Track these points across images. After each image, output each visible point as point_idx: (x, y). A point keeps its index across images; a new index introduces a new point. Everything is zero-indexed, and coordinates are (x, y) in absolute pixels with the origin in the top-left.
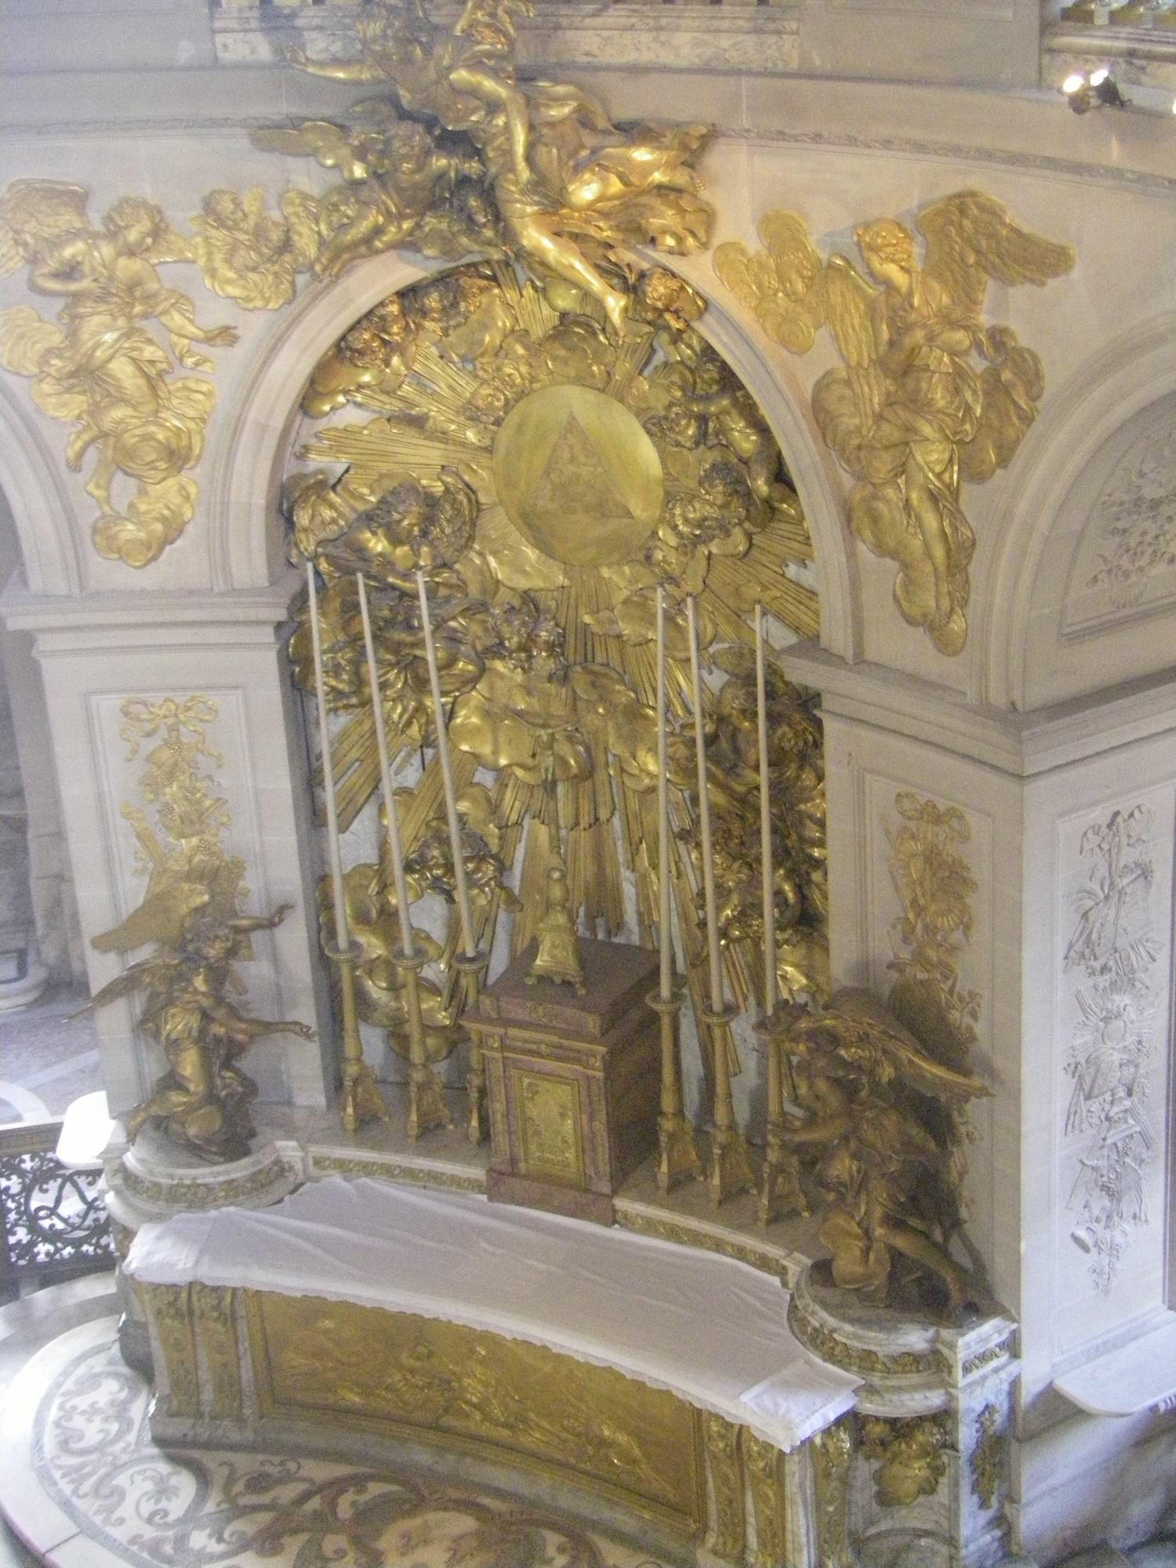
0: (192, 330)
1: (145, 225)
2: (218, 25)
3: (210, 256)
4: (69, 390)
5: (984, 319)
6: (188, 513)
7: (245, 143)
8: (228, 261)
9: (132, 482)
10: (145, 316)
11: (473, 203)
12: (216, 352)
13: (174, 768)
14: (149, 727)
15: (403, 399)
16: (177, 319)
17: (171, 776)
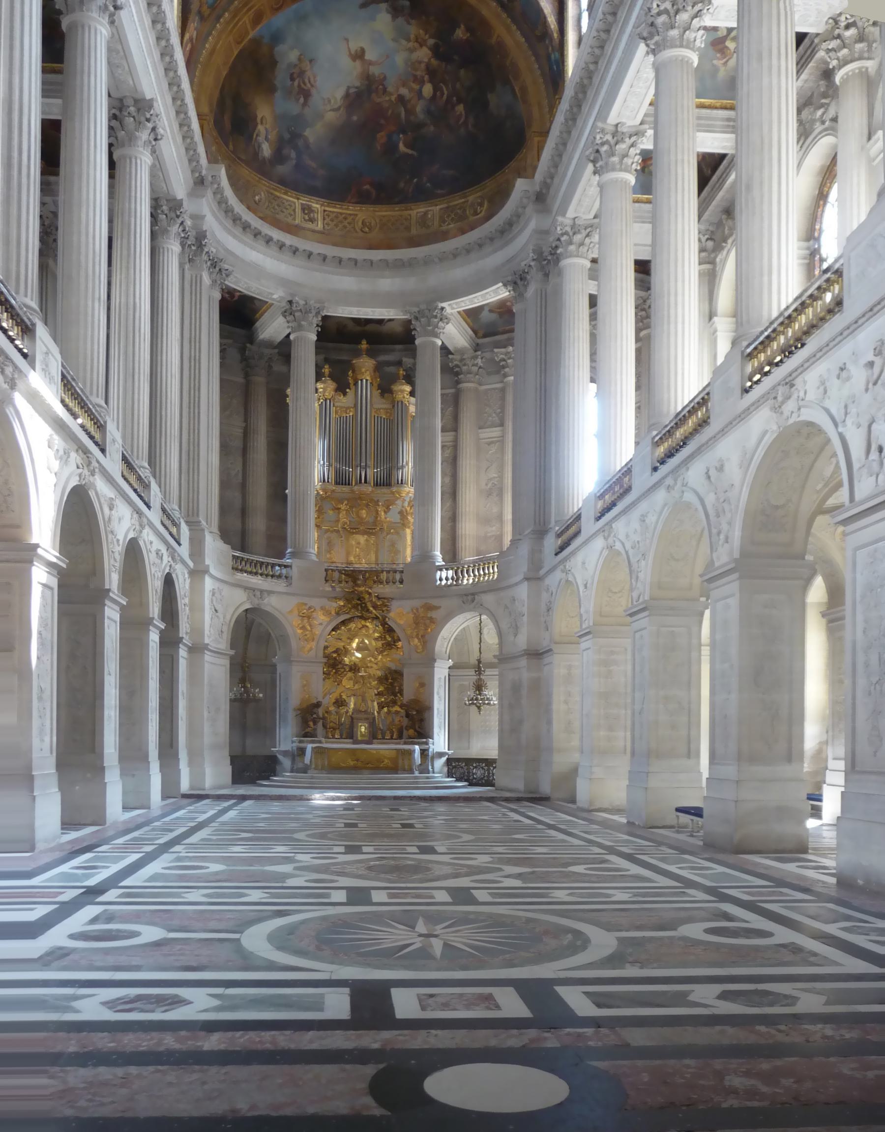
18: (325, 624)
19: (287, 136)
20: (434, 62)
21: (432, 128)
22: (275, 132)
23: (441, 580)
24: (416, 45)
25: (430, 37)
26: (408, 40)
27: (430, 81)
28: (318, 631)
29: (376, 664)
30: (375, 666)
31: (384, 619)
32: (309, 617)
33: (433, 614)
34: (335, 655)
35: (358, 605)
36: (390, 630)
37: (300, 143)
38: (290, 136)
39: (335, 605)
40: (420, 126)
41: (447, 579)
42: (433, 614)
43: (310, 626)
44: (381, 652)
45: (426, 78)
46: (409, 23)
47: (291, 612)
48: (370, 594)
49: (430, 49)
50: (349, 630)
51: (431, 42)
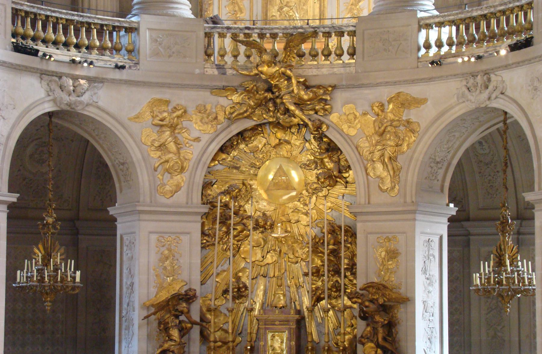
0: (189, 137)
1: (183, 110)
2: (206, 66)
3: (196, 119)
4: (157, 150)
5: (404, 118)
6: (182, 184)
7: (209, 93)
8: (201, 121)
9: (169, 175)
10: (179, 133)
11: (271, 105)
12: (195, 144)
13: (168, 258)
14: (163, 244)
15: (234, 163)
16: (186, 135)
17: (167, 258)
18: (205, 139)
23: (428, 46)
28: (192, 152)
29: (306, 214)
30: (304, 220)
31: (318, 128)
32: (173, 127)
33: (413, 115)
34: (226, 199)
36: (332, 149)
39: (223, 101)
41: (439, 45)
42: (413, 115)
43: (175, 143)
44: (316, 191)
47: (137, 117)
48: (289, 79)
50: (255, 151)
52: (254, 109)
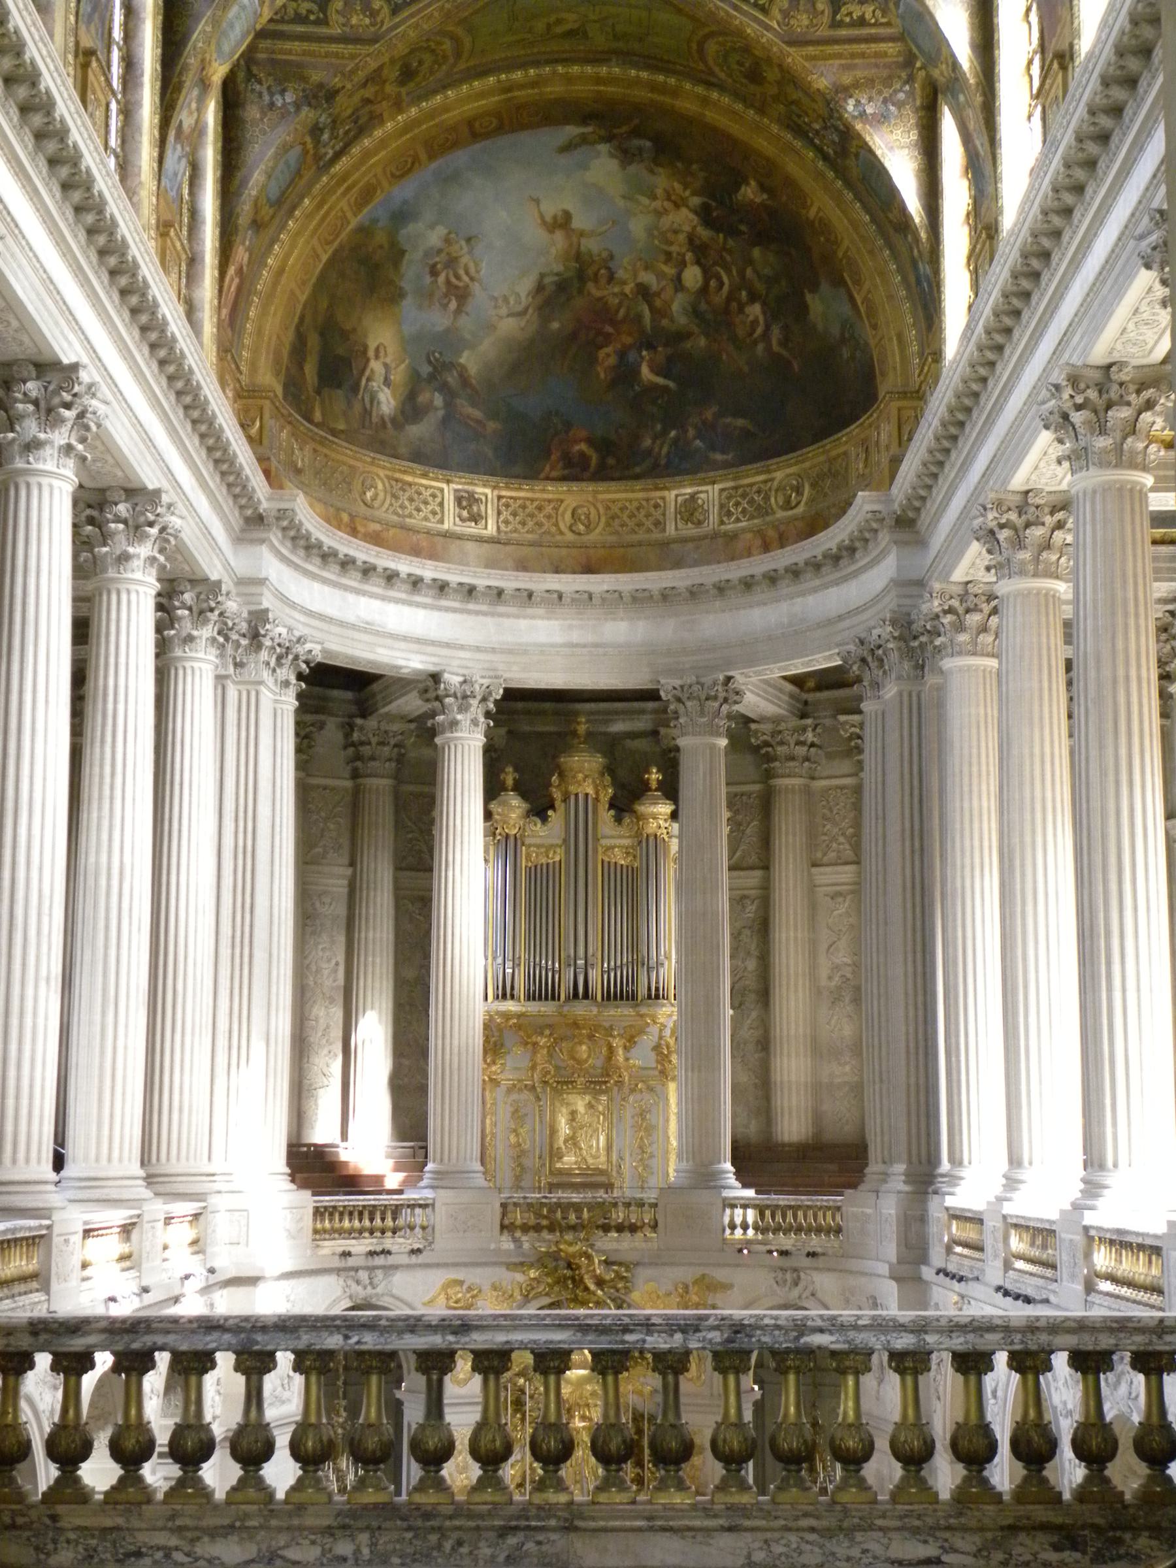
19: (426, 370)
20: (704, 233)
21: (703, 342)
22: (403, 366)
24: (666, 204)
25: (694, 194)
26: (654, 197)
27: (698, 262)
35: (565, 1278)
37: (452, 379)
38: (434, 370)
40: (682, 335)
45: (689, 256)
46: (652, 172)
49: (696, 213)
51: (696, 201)
52: (551, 1286)
